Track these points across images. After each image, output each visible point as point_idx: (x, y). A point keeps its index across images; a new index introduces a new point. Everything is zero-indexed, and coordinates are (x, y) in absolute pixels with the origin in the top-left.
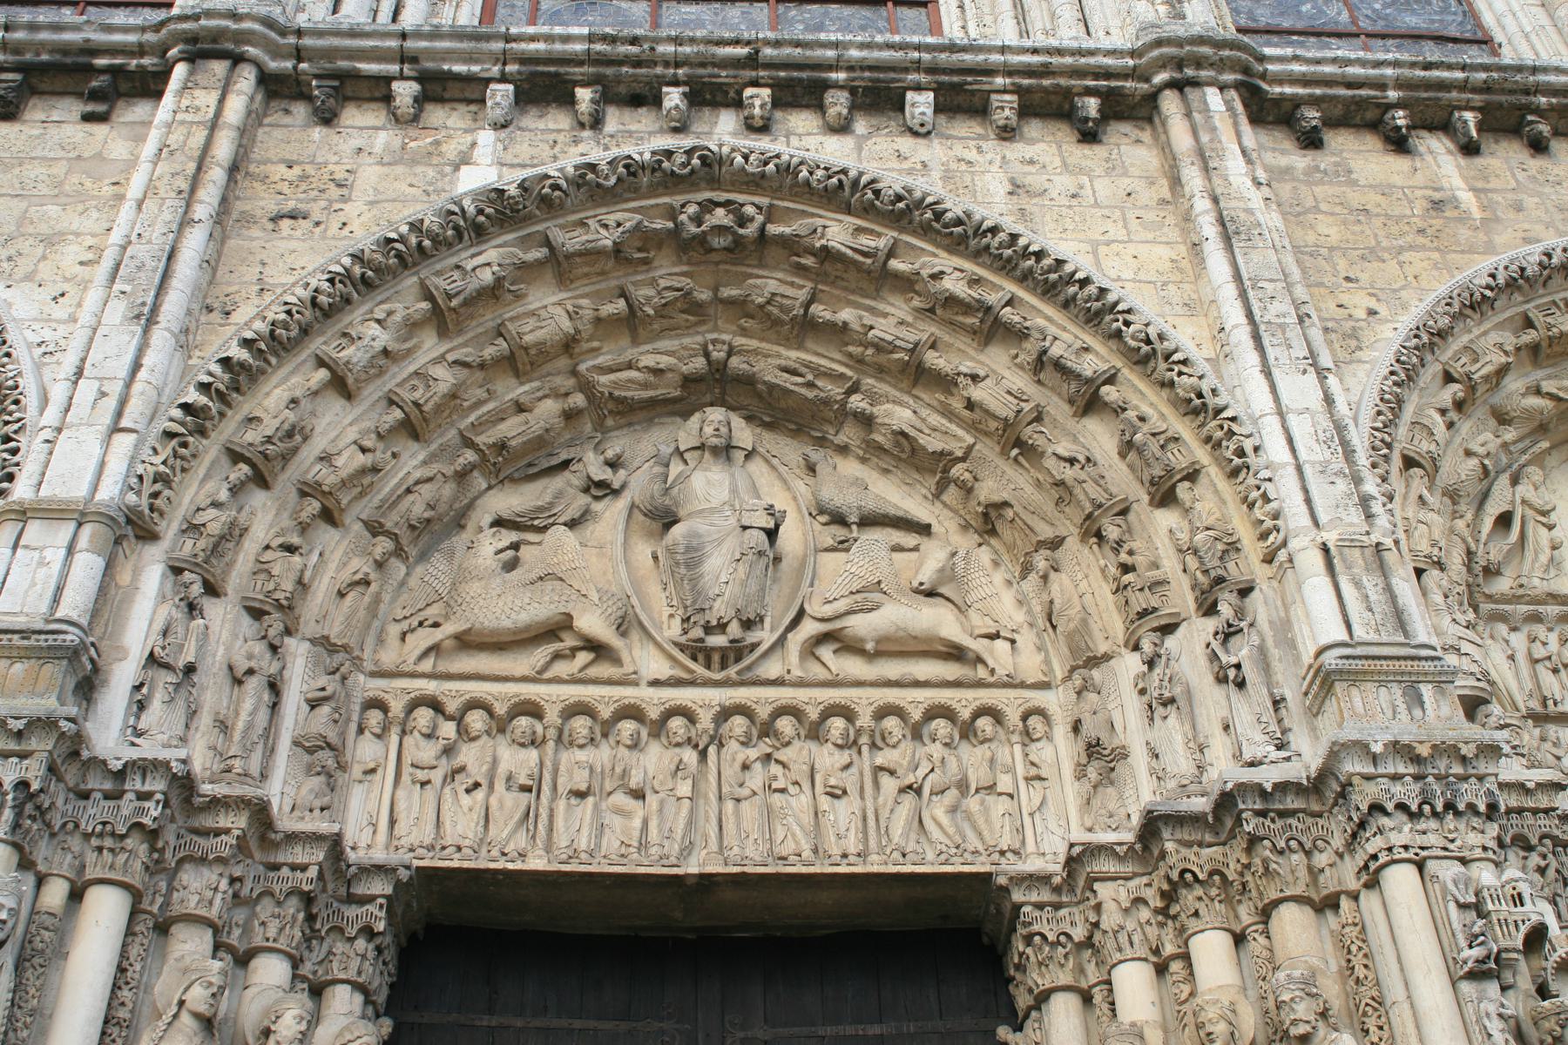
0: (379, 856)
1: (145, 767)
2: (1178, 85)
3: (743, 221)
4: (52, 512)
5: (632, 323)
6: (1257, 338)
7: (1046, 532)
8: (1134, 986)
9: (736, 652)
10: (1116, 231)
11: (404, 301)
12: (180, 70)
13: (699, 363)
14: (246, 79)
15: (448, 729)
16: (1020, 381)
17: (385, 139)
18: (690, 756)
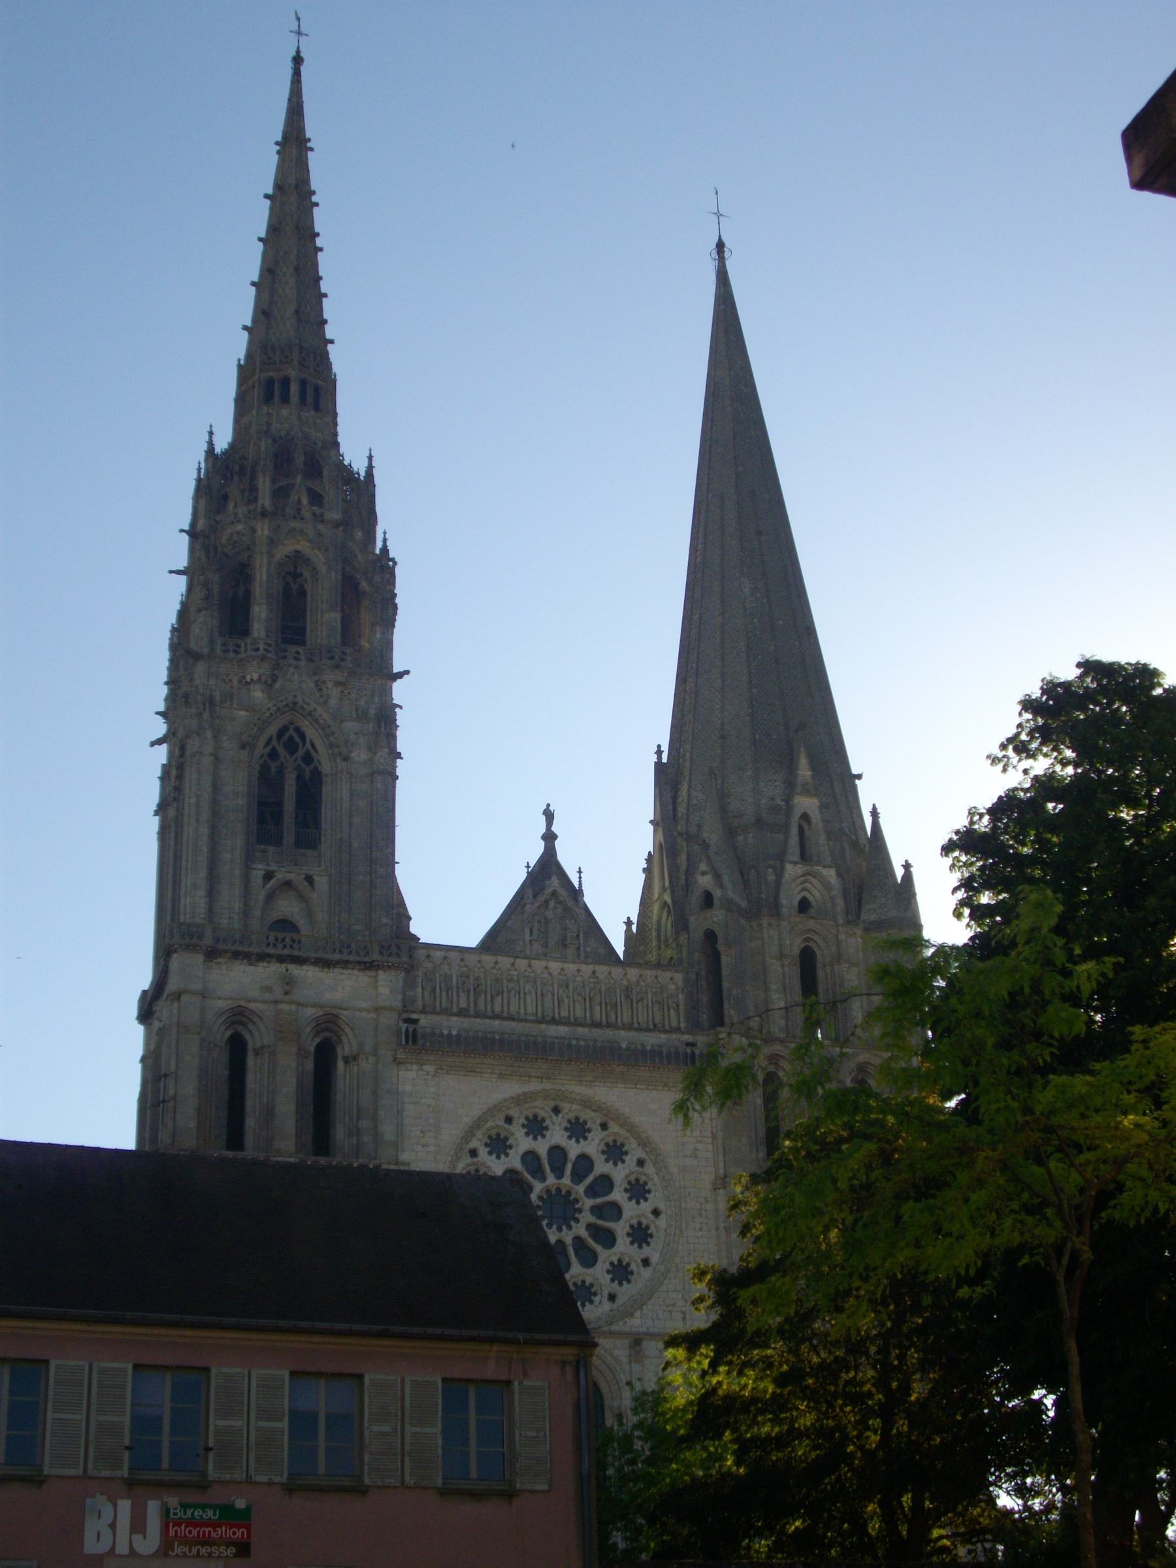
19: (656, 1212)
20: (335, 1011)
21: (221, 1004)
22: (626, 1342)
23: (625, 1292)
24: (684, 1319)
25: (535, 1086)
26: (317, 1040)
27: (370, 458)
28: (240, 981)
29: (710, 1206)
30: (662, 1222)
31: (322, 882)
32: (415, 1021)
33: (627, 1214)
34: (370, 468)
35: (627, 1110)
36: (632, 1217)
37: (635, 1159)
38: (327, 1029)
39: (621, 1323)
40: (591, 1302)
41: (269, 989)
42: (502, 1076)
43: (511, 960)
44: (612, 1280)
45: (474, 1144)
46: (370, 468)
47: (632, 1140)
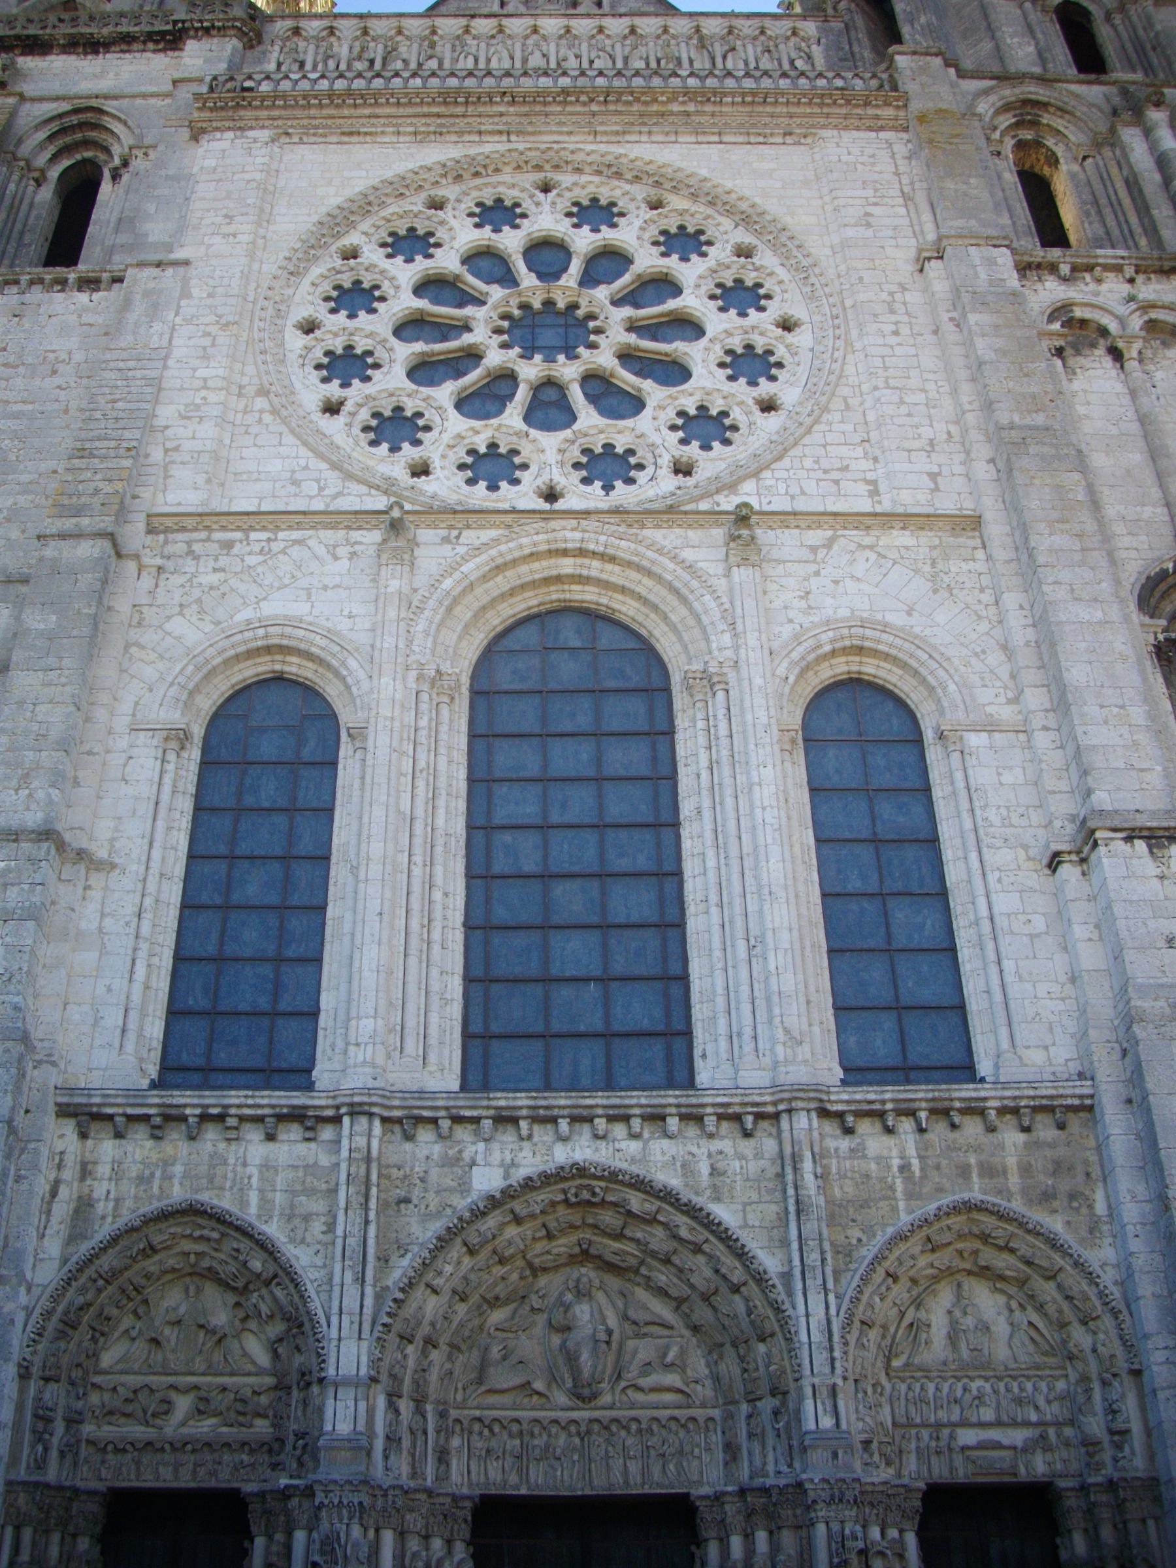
0: (465, 1491)
1: (394, 1487)
2: (789, 1111)
3: (594, 1194)
4: (347, 1382)
5: (550, 1236)
6: (803, 1273)
7: (719, 1339)
8: (736, 1542)
9: (594, 1396)
10: (754, 1196)
11: (456, 1250)
12: (346, 1120)
13: (577, 1250)
14: (377, 1123)
15: (486, 1432)
16: (708, 1273)
17: (437, 1149)
18: (577, 1441)
19: (787, 325)
20: (94, 103)
22: (718, 534)
23: (713, 463)
24: (874, 493)
25: (493, 147)
26: (66, 163)
29: (914, 298)
35: (704, 172)
36: (728, 333)
37: (729, 247)
38: (87, 143)
43: (463, 21)
44: (684, 442)
45: (353, 239)
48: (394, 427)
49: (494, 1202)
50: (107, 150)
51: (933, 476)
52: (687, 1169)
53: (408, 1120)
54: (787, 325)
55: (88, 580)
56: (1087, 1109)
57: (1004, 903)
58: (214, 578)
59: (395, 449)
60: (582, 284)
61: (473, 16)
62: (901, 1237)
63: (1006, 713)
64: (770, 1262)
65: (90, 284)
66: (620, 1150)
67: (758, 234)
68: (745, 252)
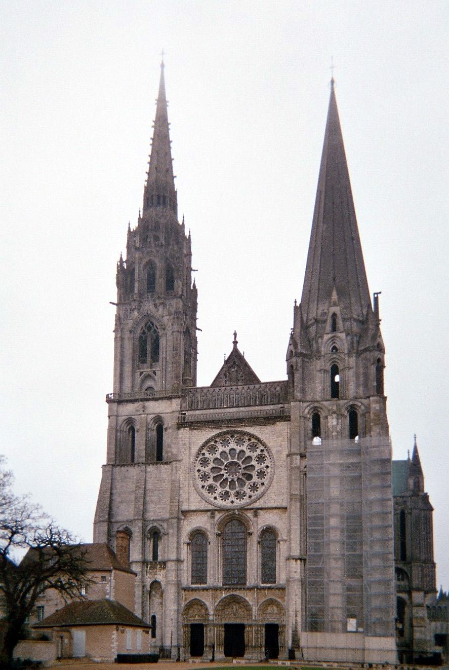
19: (267, 467)
21: (124, 418)
27: (183, 217)
28: (128, 409)
30: (269, 470)
31: (158, 373)
32: (185, 414)
33: (256, 469)
34: (183, 221)
35: (256, 434)
38: (159, 420)
39: (252, 505)
40: (243, 499)
41: (137, 411)
42: (212, 428)
46: (183, 221)
47: (259, 444)
48: (211, 489)
49: (224, 598)
50: (163, 424)
51: (283, 499)
52: (244, 594)
53: (215, 589)
54: (267, 467)
55: (176, 525)
56: (285, 589)
57: (281, 564)
58: (190, 520)
59: (212, 494)
60: (238, 459)
61: (221, 387)
62: (263, 602)
63: (285, 538)
64: (251, 603)
65: (166, 463)
66: (237, 593)
67: (265, 447)
68: (262, 451)
